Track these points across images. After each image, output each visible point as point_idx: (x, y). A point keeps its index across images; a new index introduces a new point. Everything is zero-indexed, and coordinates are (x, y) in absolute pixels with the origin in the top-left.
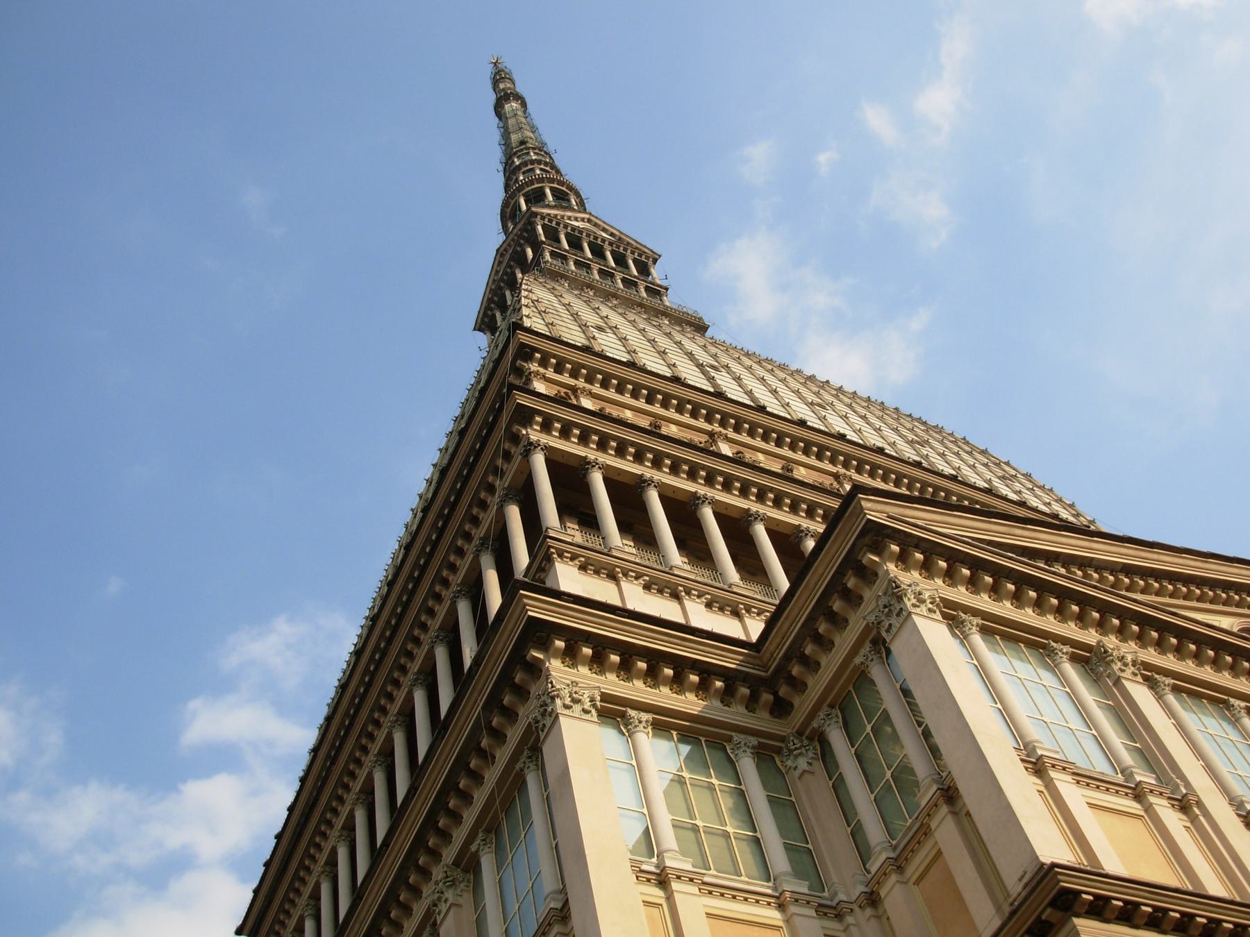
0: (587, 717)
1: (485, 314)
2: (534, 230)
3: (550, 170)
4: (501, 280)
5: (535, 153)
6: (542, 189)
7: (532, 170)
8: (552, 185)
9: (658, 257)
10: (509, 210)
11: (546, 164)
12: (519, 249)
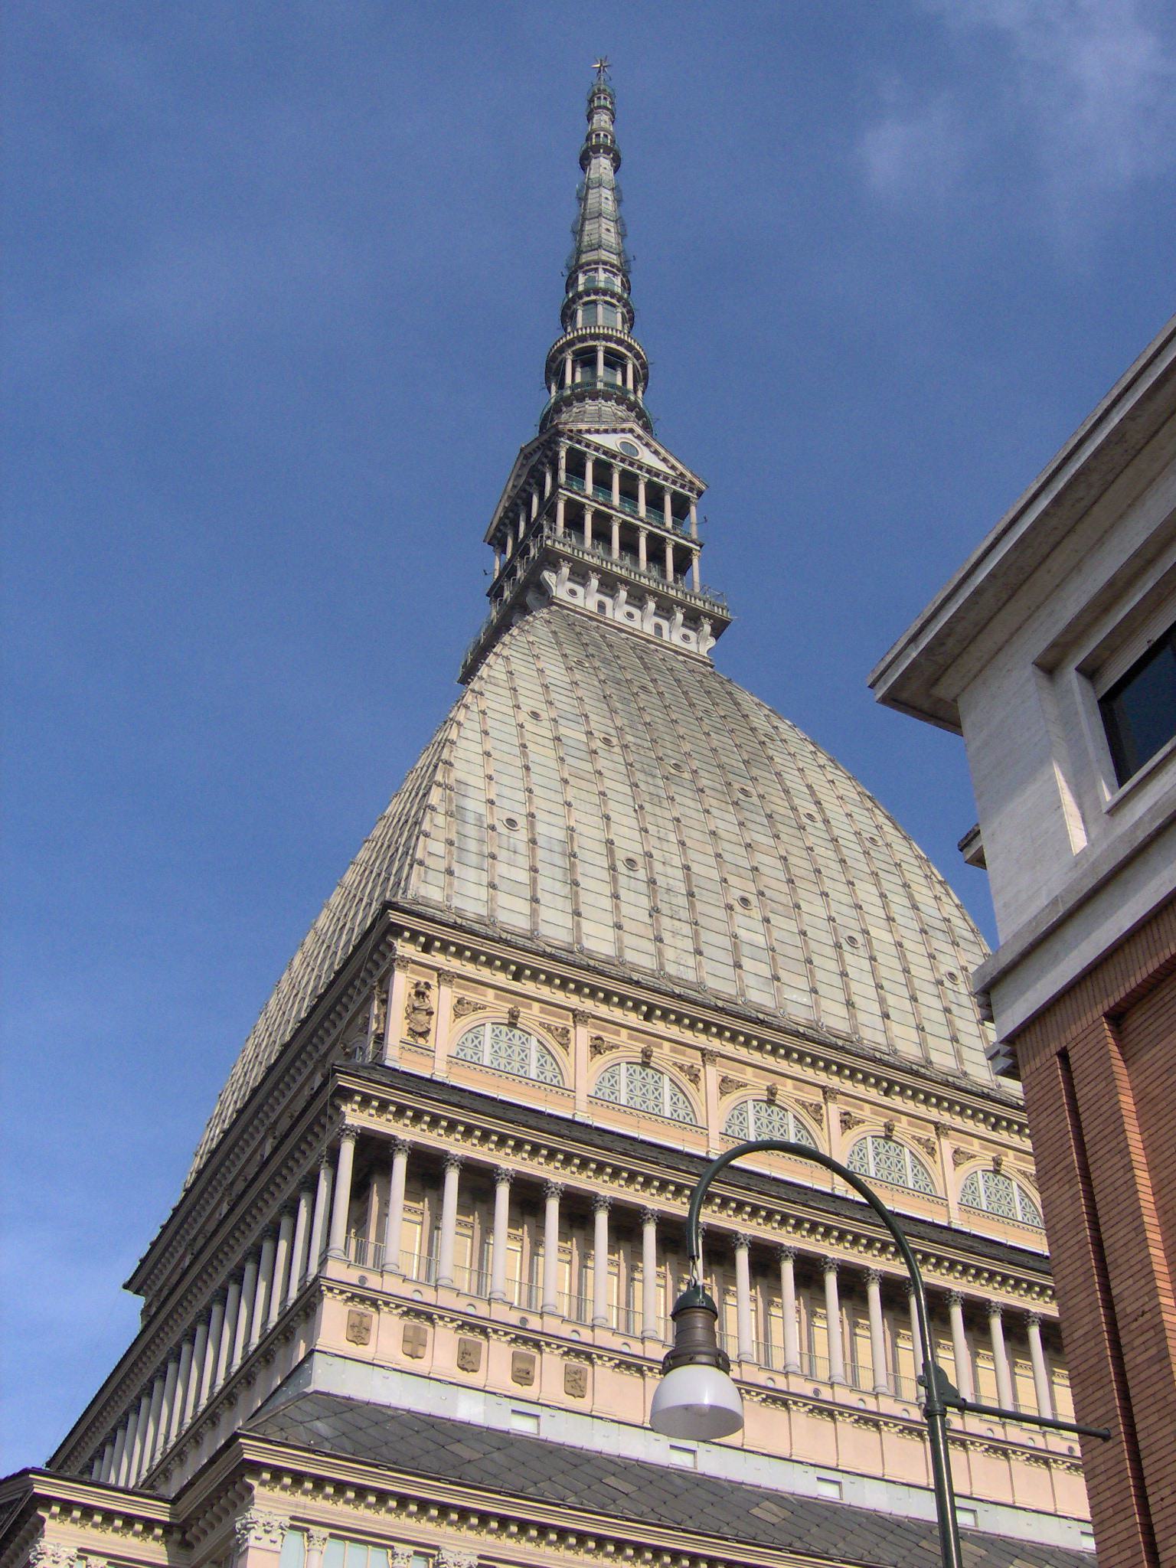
0: (272, 1546)
1: (498, 529)
2: (557, 454)
3: (617, 304)
4: (518, 495)
5: (604, 269)
6: (593, 350)
7: (594, 302)
8: (610, 345)
9: (704, 488)
10: (554, 366)
11: (613, 295)
12: (540, 467)
